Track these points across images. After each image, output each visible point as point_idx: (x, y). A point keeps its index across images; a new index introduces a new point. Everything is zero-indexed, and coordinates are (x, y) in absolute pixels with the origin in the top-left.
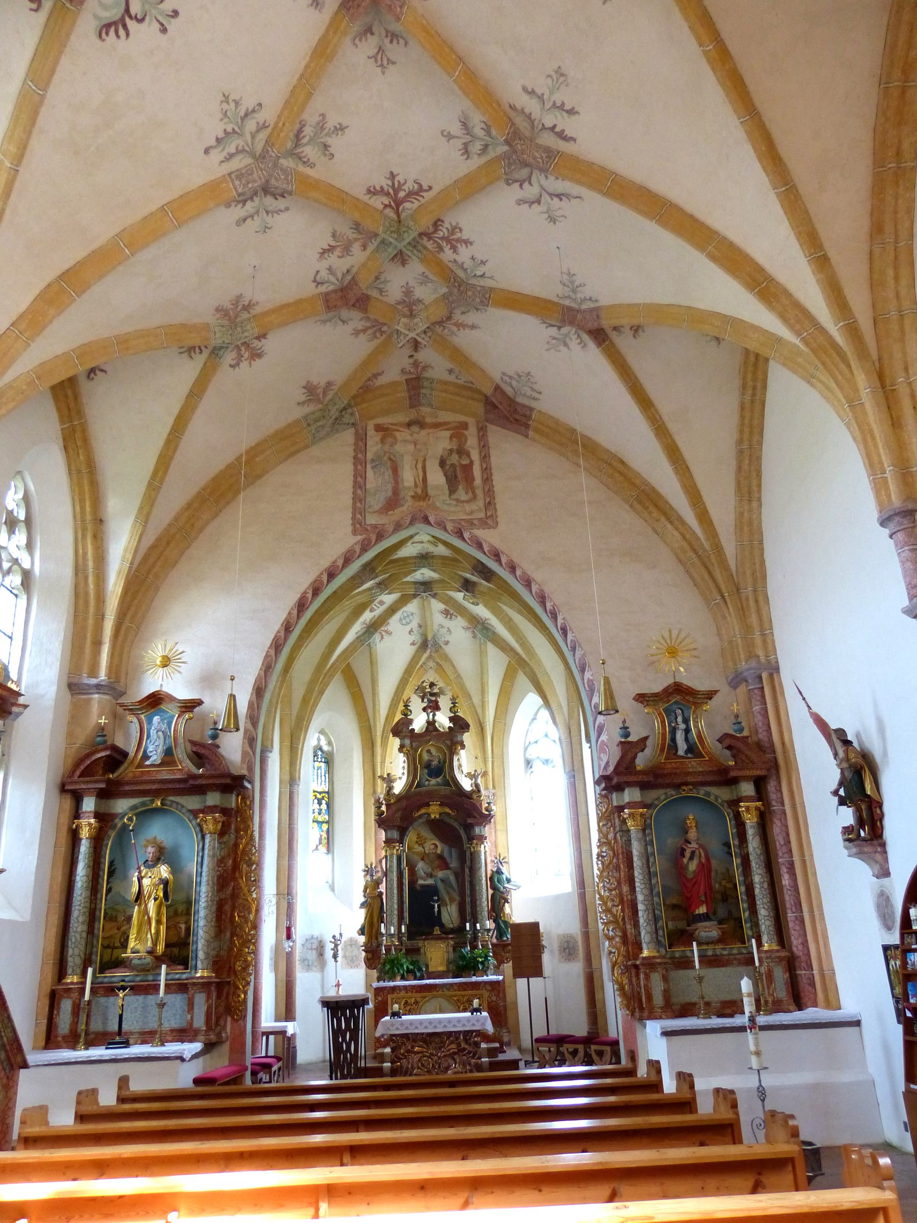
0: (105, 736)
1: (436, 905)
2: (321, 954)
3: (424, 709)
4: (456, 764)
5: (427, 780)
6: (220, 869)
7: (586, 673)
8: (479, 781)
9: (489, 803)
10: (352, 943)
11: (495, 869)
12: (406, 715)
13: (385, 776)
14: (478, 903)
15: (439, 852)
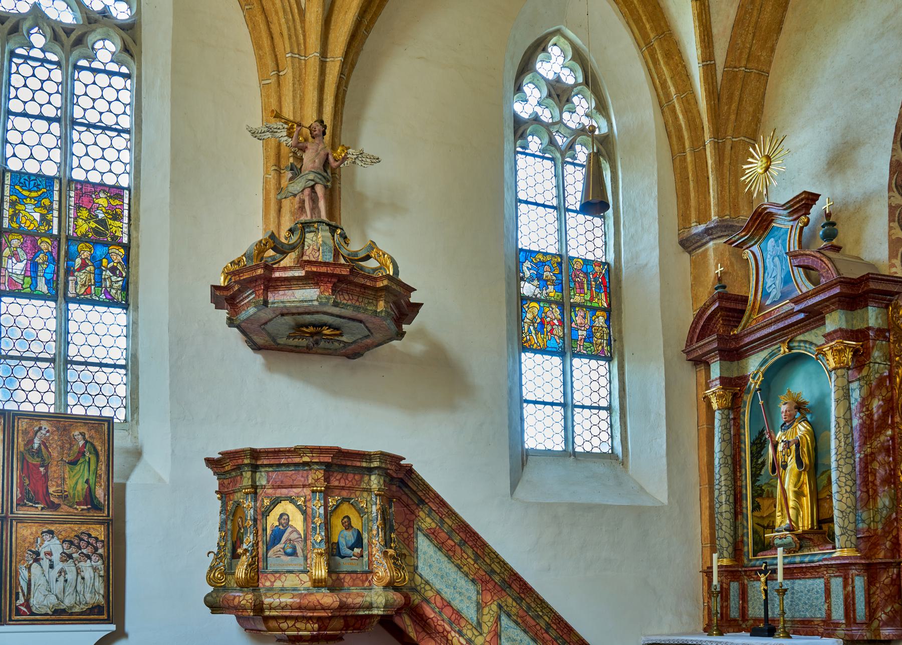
0: (724, 287)
6: (862, 415)
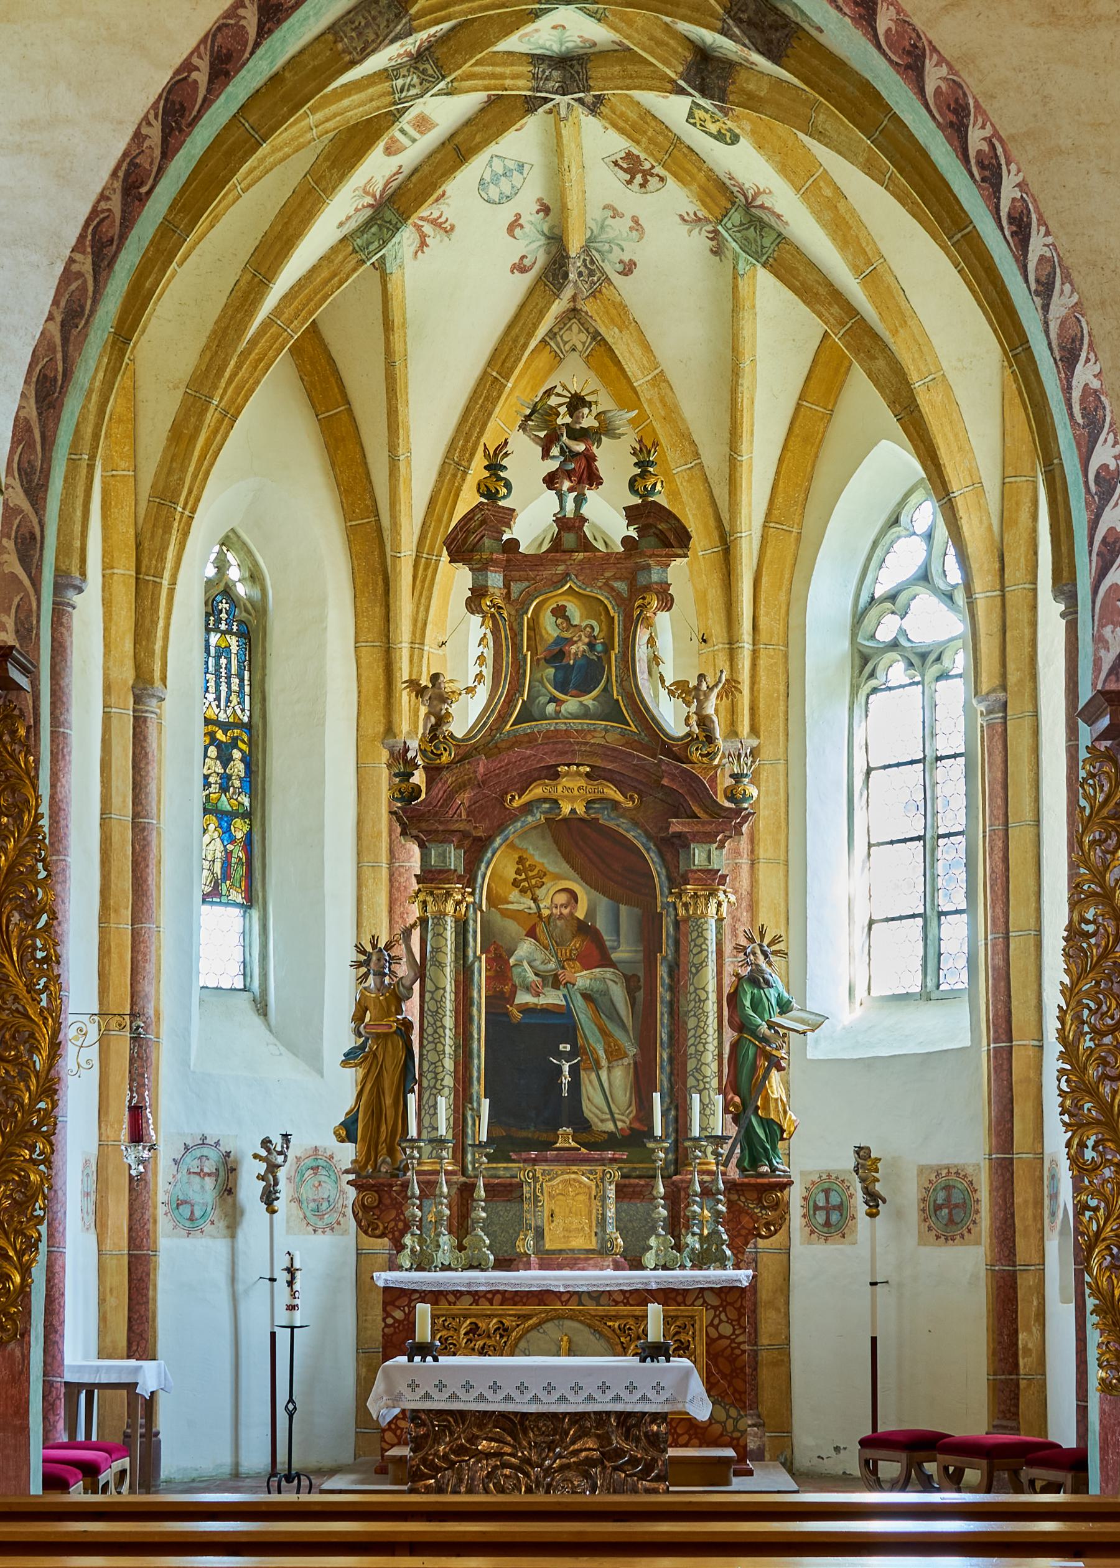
1: (566, 1068)
2: (228, 1190)
3: (551, 481)
4: (642, 652)
5: (554, 699)
7: (1079, 367)
8: (710, 709)
9: (737, 777)
10: (318, 1162)
11: (745, 972)
12: (491, 495)
13: (425, 681)
14: (691, 1065)
15: (580, 914)
